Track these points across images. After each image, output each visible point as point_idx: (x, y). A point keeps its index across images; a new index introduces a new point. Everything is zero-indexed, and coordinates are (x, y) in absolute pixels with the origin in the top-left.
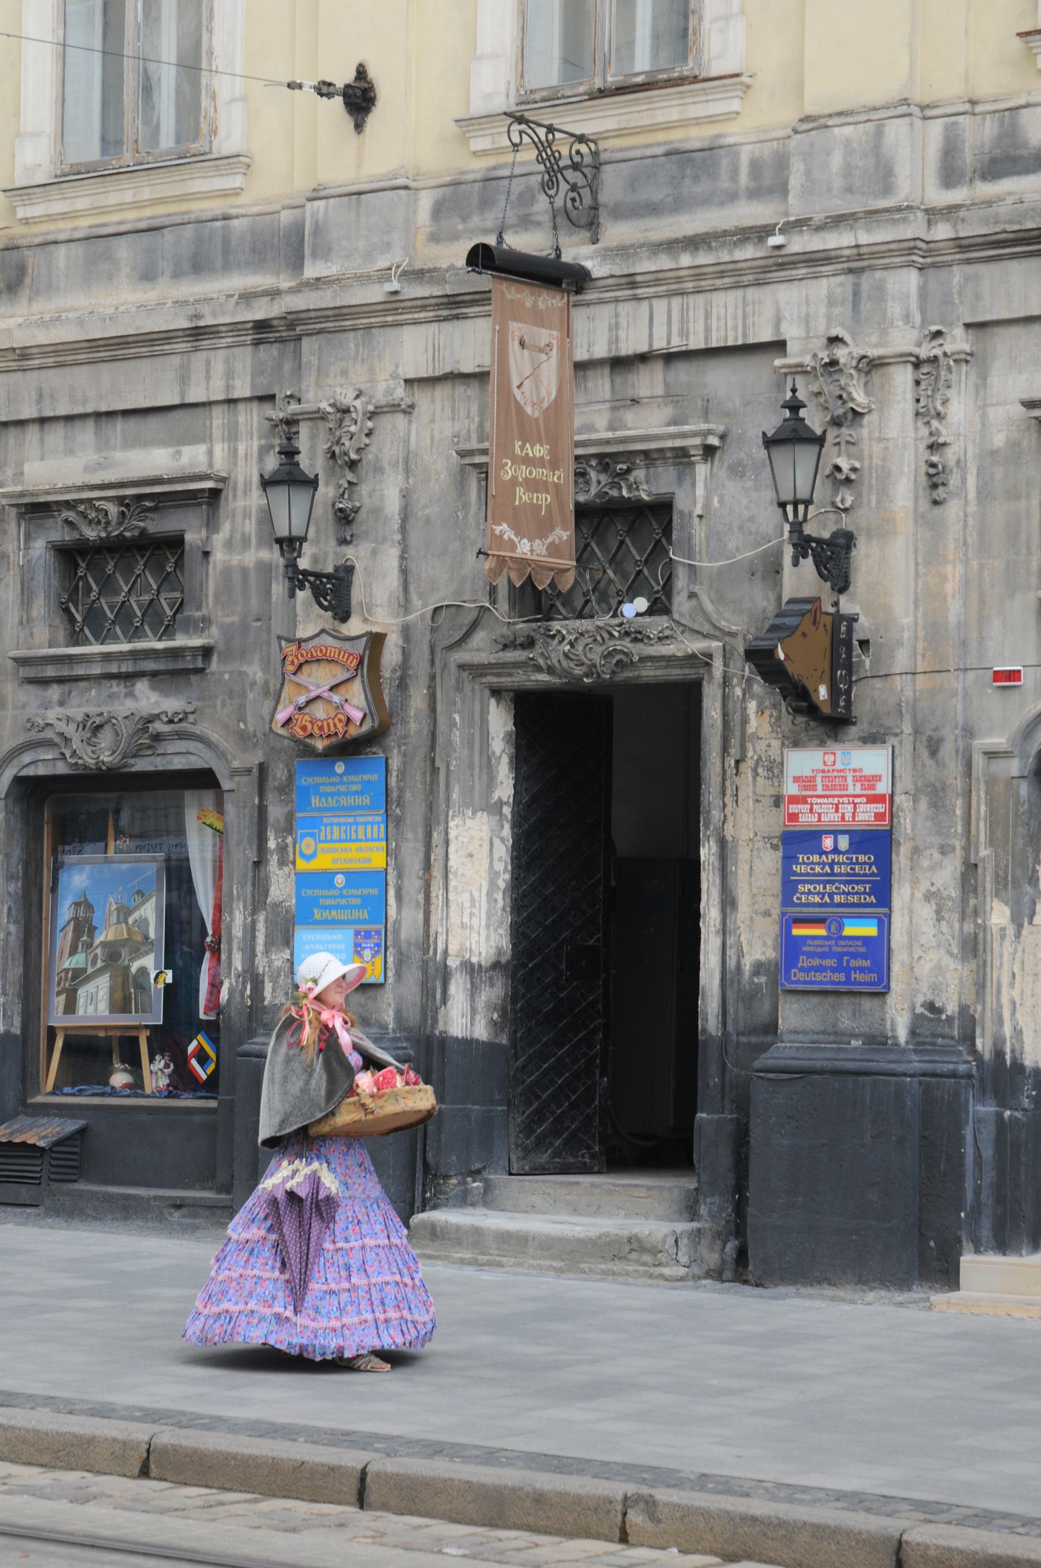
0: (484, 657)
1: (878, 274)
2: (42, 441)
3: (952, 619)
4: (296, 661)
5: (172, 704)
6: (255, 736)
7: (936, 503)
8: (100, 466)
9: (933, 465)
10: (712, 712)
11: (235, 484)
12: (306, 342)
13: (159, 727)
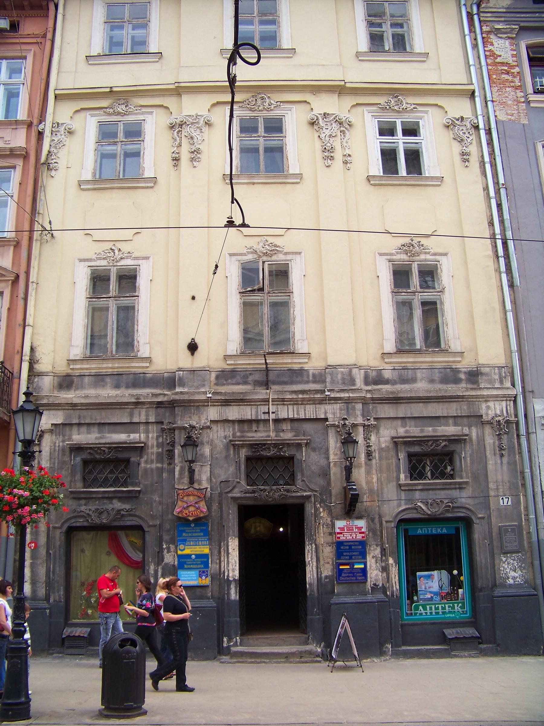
0: (238, 495)
1: (353, 404)
2: (79, 430)
3: (376, 488)
5: (127, 506)
7: (370, 460)
8: (101, 438)
9: (369, 451)
13: (122, 512)
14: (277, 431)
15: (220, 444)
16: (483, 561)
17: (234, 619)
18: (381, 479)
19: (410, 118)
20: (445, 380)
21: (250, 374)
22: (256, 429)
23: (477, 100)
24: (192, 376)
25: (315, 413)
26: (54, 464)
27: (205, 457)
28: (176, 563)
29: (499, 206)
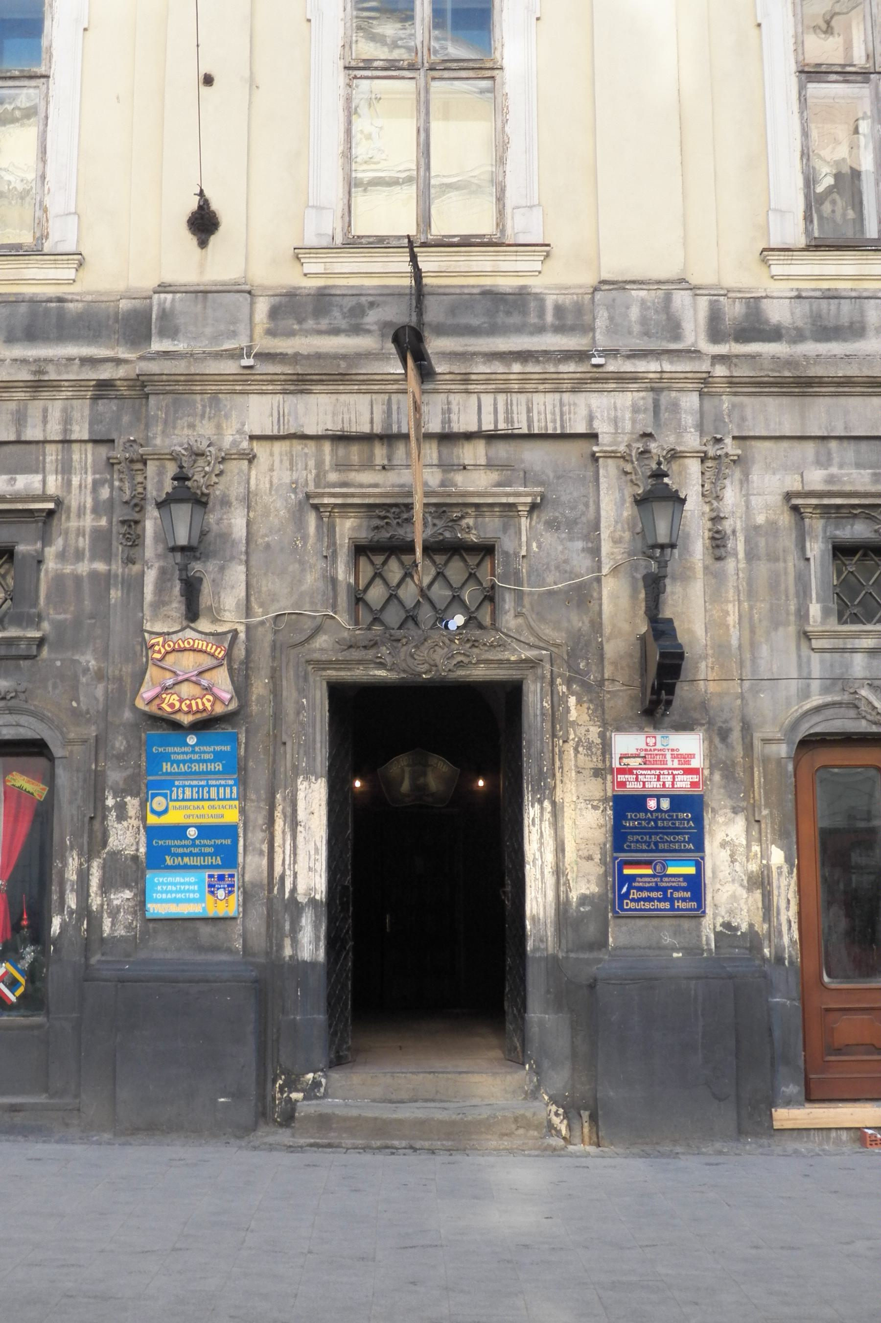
1: (673, 394)
3: (734, 642)
4: (163, 651)
6: (88, 712)
7: (719, 559)
9: (718, 532)
11: (69, 508)
12: (152, 400)
14: (446, 466)
18: (751, 618)
21: (372, 305)
22: (386, 462)
24: (200, 306)
25: (558, 418)
27: (234, 544)
28: (143, 850)
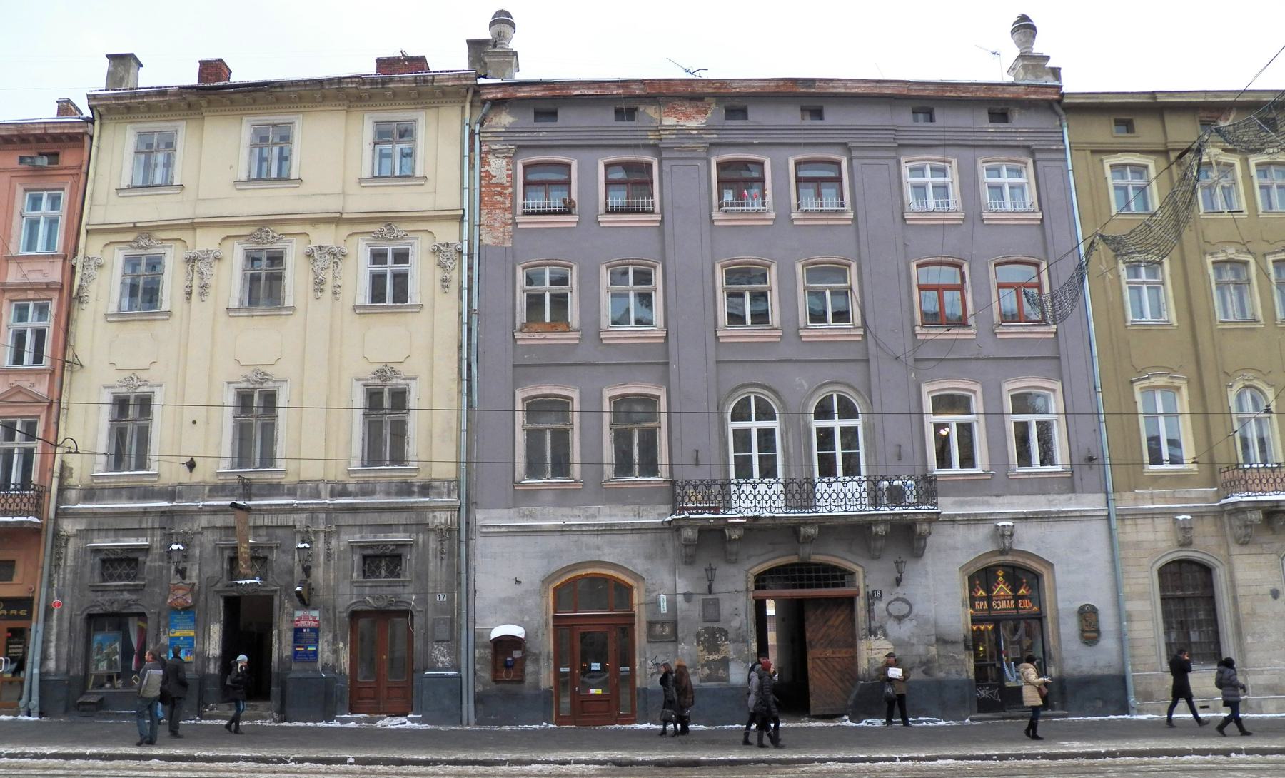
0: (221, 589)
10: (276, 602)
13: (130, 602)
15: (209, 547)
16: (419, 647)
17: (213, 689)
19: (399, 245)
20: (400, 493)
23: (466, 224)
26: (78, 562)
29: (469, 330)
